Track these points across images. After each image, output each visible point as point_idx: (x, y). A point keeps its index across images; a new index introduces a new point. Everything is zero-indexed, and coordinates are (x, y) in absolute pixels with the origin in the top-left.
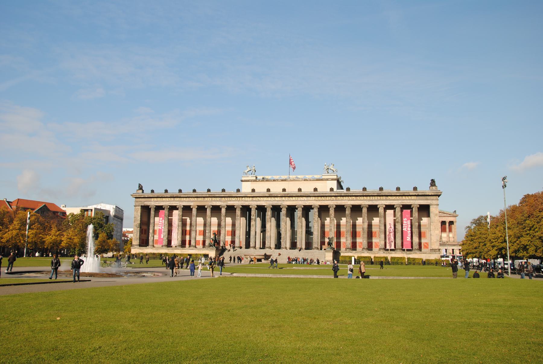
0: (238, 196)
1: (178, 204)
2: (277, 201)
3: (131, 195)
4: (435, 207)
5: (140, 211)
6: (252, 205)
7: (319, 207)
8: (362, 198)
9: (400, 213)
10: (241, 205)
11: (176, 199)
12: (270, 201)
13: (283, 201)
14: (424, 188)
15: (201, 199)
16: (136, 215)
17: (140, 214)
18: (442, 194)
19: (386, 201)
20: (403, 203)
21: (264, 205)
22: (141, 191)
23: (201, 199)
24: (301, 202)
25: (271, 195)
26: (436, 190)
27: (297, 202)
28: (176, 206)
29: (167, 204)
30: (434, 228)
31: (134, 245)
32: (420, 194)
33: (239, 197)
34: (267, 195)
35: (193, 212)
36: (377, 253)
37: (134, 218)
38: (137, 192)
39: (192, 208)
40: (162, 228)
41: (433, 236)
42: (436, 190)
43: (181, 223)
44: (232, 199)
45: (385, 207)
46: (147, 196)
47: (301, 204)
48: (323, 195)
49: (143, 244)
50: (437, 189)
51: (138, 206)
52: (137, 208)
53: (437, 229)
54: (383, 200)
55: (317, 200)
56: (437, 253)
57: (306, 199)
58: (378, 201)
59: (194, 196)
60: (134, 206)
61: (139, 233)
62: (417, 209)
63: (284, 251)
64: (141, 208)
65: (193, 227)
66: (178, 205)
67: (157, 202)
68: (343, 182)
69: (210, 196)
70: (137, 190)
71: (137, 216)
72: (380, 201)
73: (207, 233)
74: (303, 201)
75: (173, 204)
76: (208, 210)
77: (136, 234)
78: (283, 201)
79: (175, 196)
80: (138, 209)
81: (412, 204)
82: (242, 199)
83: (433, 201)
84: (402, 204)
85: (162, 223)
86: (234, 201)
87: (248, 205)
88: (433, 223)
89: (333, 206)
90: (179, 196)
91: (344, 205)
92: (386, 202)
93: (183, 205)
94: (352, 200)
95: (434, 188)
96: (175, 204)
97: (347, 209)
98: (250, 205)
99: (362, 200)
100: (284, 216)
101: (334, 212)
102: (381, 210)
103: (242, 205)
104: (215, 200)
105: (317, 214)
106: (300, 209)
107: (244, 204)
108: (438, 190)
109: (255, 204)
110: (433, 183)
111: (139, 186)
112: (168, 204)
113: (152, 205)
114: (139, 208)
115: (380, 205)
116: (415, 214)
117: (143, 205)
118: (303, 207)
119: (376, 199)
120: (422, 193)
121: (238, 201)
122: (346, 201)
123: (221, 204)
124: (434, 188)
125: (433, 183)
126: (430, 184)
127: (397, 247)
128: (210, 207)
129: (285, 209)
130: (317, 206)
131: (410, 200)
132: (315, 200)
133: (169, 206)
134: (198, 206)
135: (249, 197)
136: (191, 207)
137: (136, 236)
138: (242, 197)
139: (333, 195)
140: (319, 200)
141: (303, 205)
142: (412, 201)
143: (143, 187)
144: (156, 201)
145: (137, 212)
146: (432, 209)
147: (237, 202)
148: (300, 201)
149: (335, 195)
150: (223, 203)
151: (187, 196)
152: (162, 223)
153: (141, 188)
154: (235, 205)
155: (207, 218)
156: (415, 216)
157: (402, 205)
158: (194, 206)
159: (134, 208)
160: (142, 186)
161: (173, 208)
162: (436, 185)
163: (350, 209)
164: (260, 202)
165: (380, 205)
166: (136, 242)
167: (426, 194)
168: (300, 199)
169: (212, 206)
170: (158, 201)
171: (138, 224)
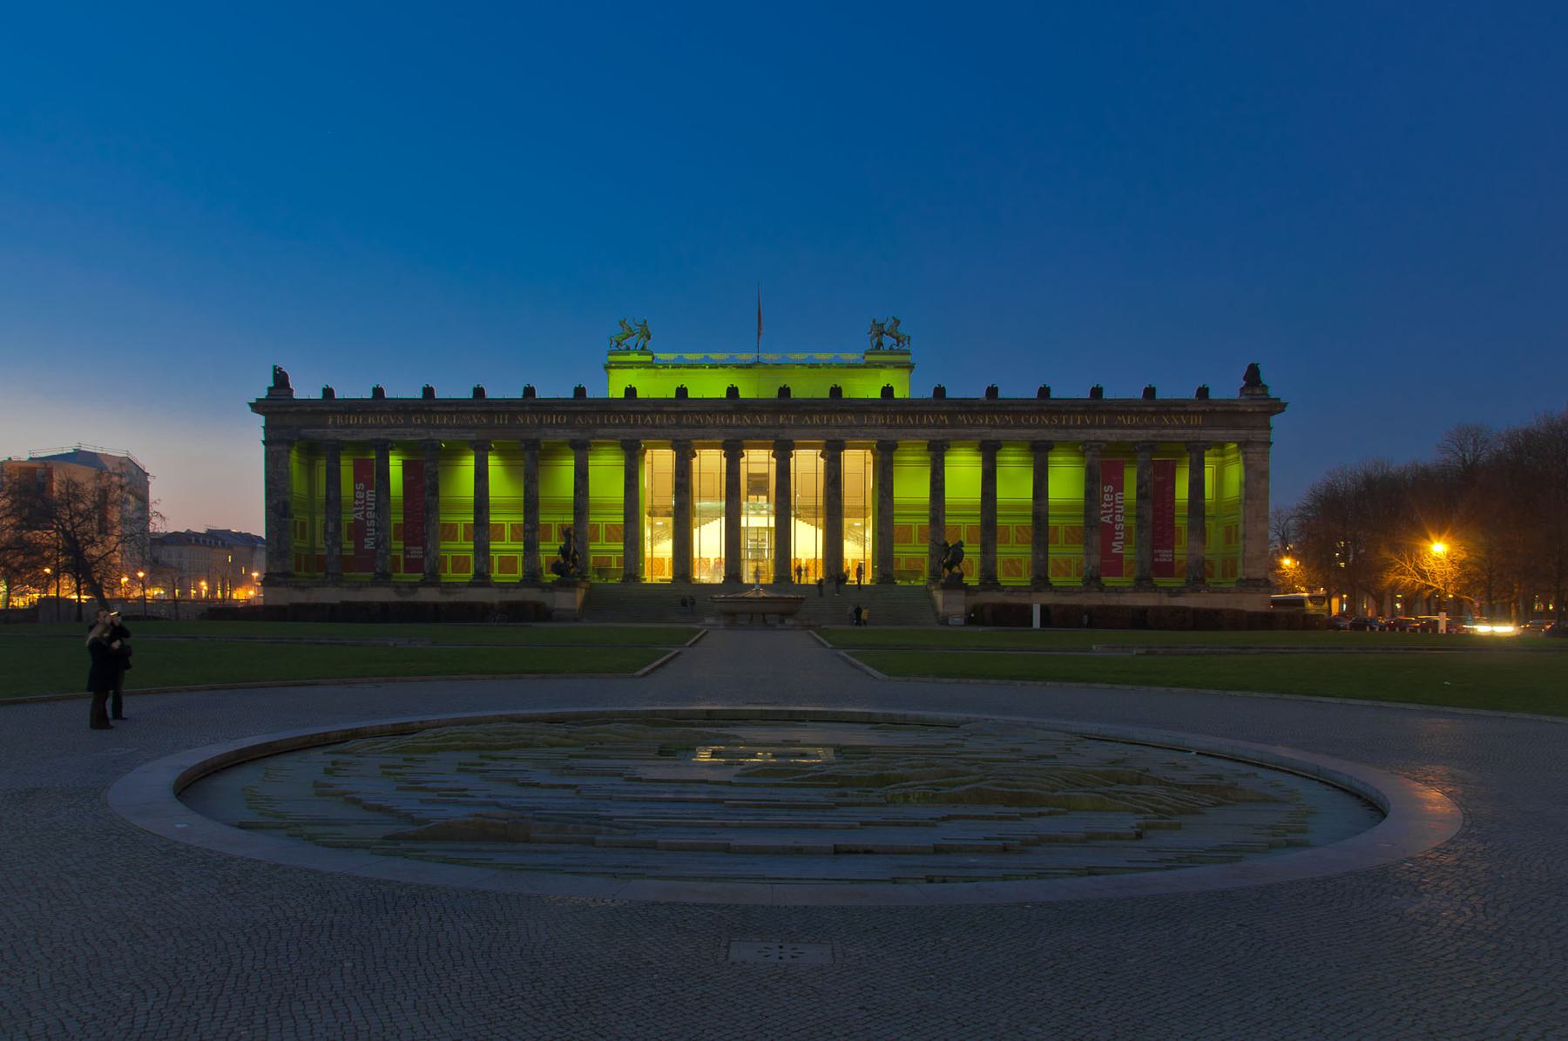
0: (631, 409)
2: (762, 427)
3: (251, 405)
4: (1259, 449)
8: (1034, 420)
11: (416, 419)
12: (738, 426)
13: (782, 426)
14: (1227, 388)
15: (504, 420)
18: (1286, 409)
19: (1112, 431)
20: (1162, 436)
23: (504, 420)
24: (838, 431)
26: (1264, 396)
27: (825, 430)
29: (382, 437)
32: (1218, 409)
33: (634, 412)
40: (364, 516)
42: (1264, 396)
44: (608, 420)
46: (309, 409)
48: (912, 408)
49: (300, 571)
50: (1267, 395)
54: (1101, 427)
55: (890, 427)
57: (855, 423)
58: (1084, 430)
59: (478, 409)
60: (263, 442)
67: (348, 431)
70: (270, 389)
72: (1092, 431)
74: (844, 427)
78: (782, 426)
79: (411, 409)
81: (1191, 439)
82: (642, 420)
83: (1256, 432)
85: (366, 502)
86: (616, 426)
92: (1111, 434)
94: (1003, 427)
96: (411, 435)
99: (1035, 427)
104: (552, 421)
108: (1272, 397)
110: (1253, 376)
111: (276, 377)
114: (280, 448)
115: (1094, 444)
119: (1079, 422)
120: (1225, 405)
121: (632, 427)
122: (984, 430)
124: (1258, 392)
125: (1253, 376)
126: (1244, 379)
131: (1182, 427)
132: (884, 425)
135: (669, 413)
138: (645, 413)
140: (900, 427)
142: (1190, 431)
144: (341, 427)
146: (1252, 455)
147: (630, 430)
148: (838, 427)
149: (950, 408)
150: (578, 434)
151: (453, 409)
152: (366, 502)
153: (281, 379)
159: (263, 448)
160: (285, 375)
164: (705, 430)
165: (1094, 444)
168: (836, 420)
170: (349, 426)
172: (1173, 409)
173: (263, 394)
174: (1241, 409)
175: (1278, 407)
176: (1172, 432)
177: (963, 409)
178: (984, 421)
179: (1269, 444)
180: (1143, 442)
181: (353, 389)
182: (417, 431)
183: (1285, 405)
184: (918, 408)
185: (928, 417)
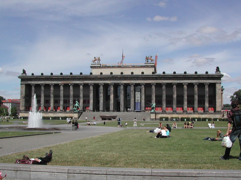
1: (50, 82)
3: (19, 77)
4: (219, 84)
5: (25, 87)
6: (101, 83)
7: (145, 84)
9: (197, 88)
10: (94, 84)
14: (212, 72)
16: (22, 90)
17: (24, 90)
20: (199, 81)
21: (108, 83)
22: (25, 74)
25: (113, 77)
26: (220, 73)
28: (49, 84)
30: (218, 98)
31: (21, 110)
32: (210, 76)
34: (110, 77)
35: (61, 88)
36: (183, 114)
37: (21, 92)
38: (22, 75)
39: (60, 86)
41: (217, 103)
42: (220, 73)
43: (53, 95)
45: (188, 84)
46: (29, 78)
47: (133, 83)
48: (147, 76)
51: (23, 84)
52: (22, 85)
53: (220, 98)
56: (220, 113)
60: (21, 84)
61: (24, 102)
62: (208, 86)
63: (122, 113)
64: (25, 86)
65: (61, 98)
66: (51, 83)
69: (73, 77)
70: (22, 74)
71: (23, 91)
72: (185, 81)
73: (71, 102)
75: (47, 82)
76: (71, 87)
77: (22, 103)
79: (48, 77)
80: (23, 86)
84: (198, 82)
87: (98, 83)
88: (217, 94)
89: (154, 84)
90: (51, 77)
91: (161, 83)
93: (54, 84)
95: (218, 72)
96: (48, 82)
97: (163, 86)
98: (99, 83)
101: (155, 88)
102: (185, 87)
103: (94, 83)
105: (144, 89)
106: (132, 86)
107: (95, 83)
108: (221, 73)
109: (102, 83)
111: (23, 71)
112: (44, 82)
113: (33, 83)
114: (23, 85)
116: (206, 89)
117: (26, 83)
123: (80, 83)
125: (218, 69)
127: (195, 110)
128: (72, 84)
129: (123, 86)
130: (143, 84)
133: (45, 84)
134: (64, 84)
136: (60, 85)
137: (22, 104)
139: (154, 76)
141: (135, 83)
143: (26, 71)
145: (23, 88)
147: (91, 81)
149: (155, 76)
153: (24, 72)
154: (89, 83)
155: (70, 92)
156: (207, 90)
157: (199, 83)
158: (61, 84)
159: (20, 85)
160: (25, 71)
161: (47, 86)
162: (220, 70)
163: (165, 86)
166: (22, 108)
167: (213, 76)
169: (74, 84)
171: (23, 96)
172: (200, 76)
173: (21, 75)
174: (214, 76)
175: (222, 76)
176: (201, 81)
177: (158, 76)
178: (163, 79)
179: (221, 83)
180: (195, 83)
181: (37, 73)
182: (50, 82)
183: (223, 75)
184: (149, 76)
185: (151, 78)
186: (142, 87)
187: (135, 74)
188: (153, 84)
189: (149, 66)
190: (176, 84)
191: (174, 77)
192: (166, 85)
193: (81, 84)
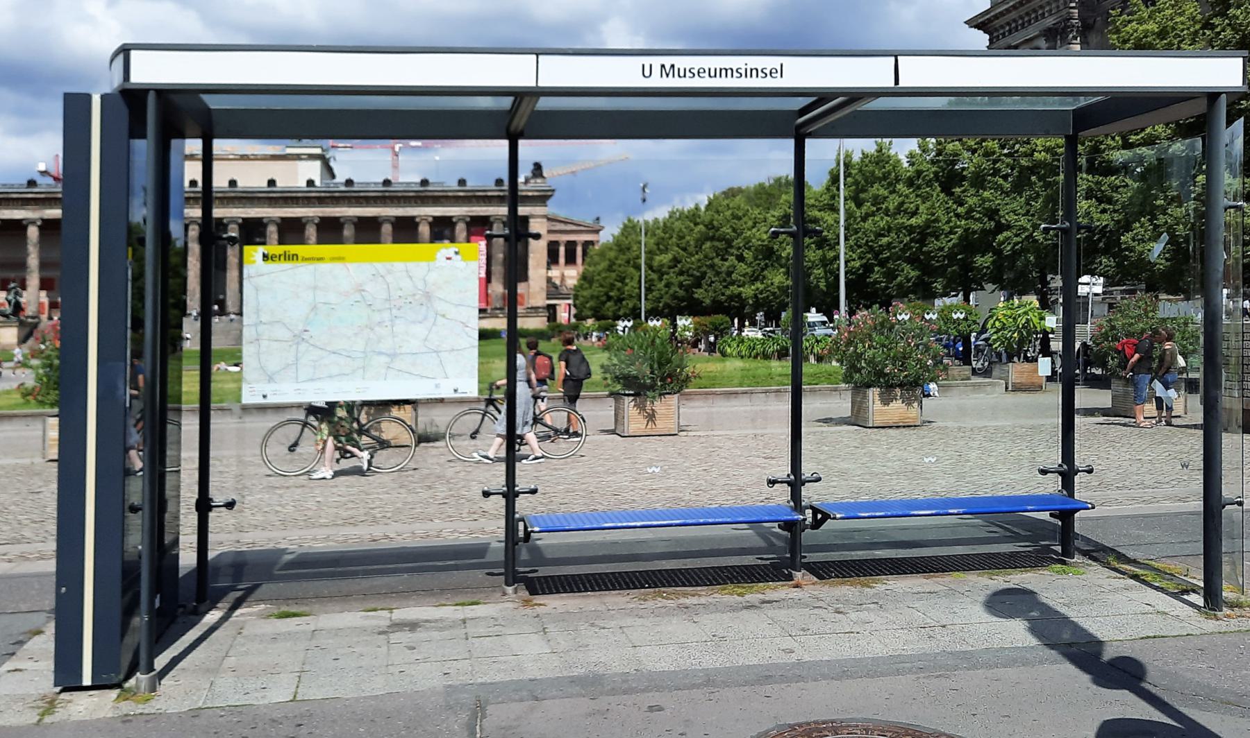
4: (539, 220)
20: (472, 211)
68: (335, 159)
84: (470, 214)
89: (312, 221)
97: (346, 226)
100: (193, 241)
102: (424, 230)
118: (240, 221)
126: (533, 172)
129: (197, 227)
130: (274, 221)
163: (352, 226)
177: (328, 195)
186: (271, 232)
187: (242, 184)
188: (309, 220)
189: (303, 157)
190: (393, 219)
191: (384, 197)
192: (355, 224)
193: (33, 222)
